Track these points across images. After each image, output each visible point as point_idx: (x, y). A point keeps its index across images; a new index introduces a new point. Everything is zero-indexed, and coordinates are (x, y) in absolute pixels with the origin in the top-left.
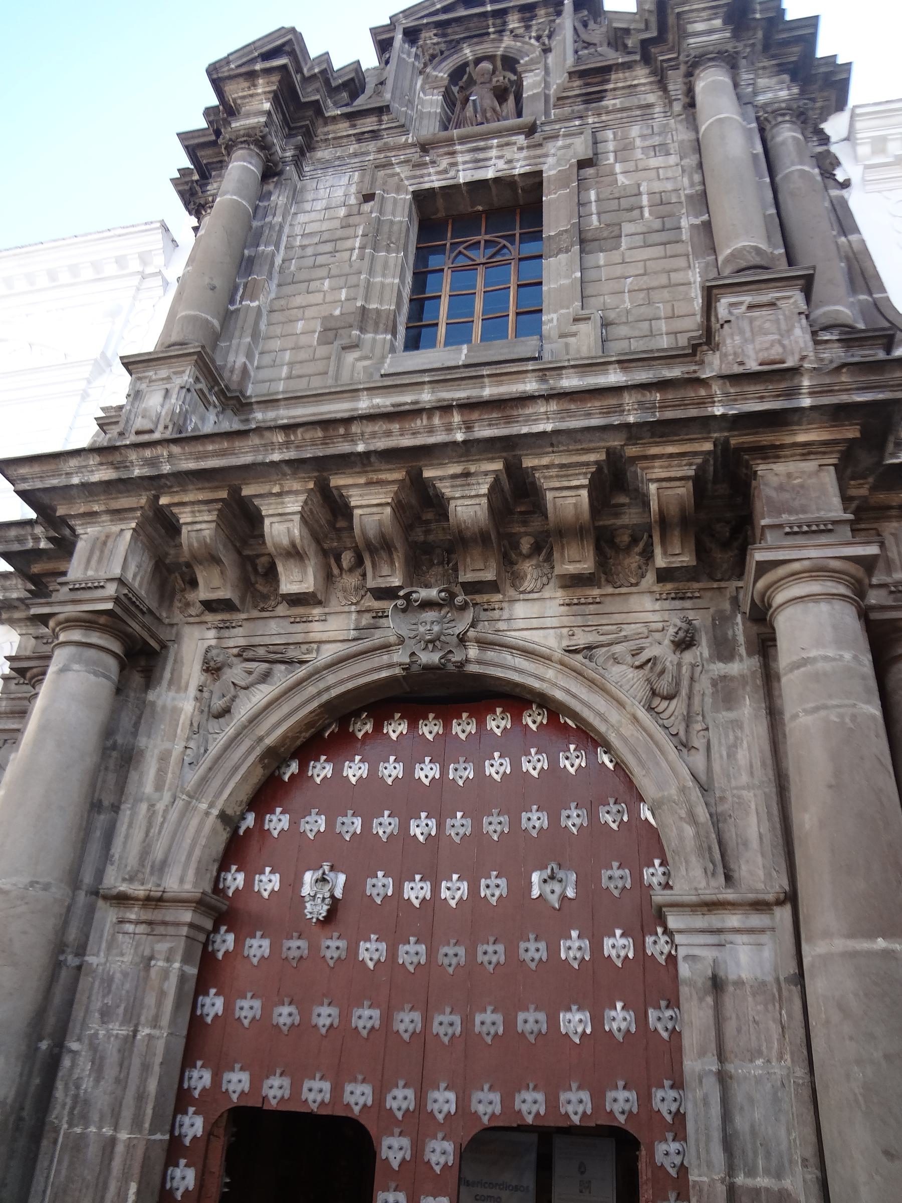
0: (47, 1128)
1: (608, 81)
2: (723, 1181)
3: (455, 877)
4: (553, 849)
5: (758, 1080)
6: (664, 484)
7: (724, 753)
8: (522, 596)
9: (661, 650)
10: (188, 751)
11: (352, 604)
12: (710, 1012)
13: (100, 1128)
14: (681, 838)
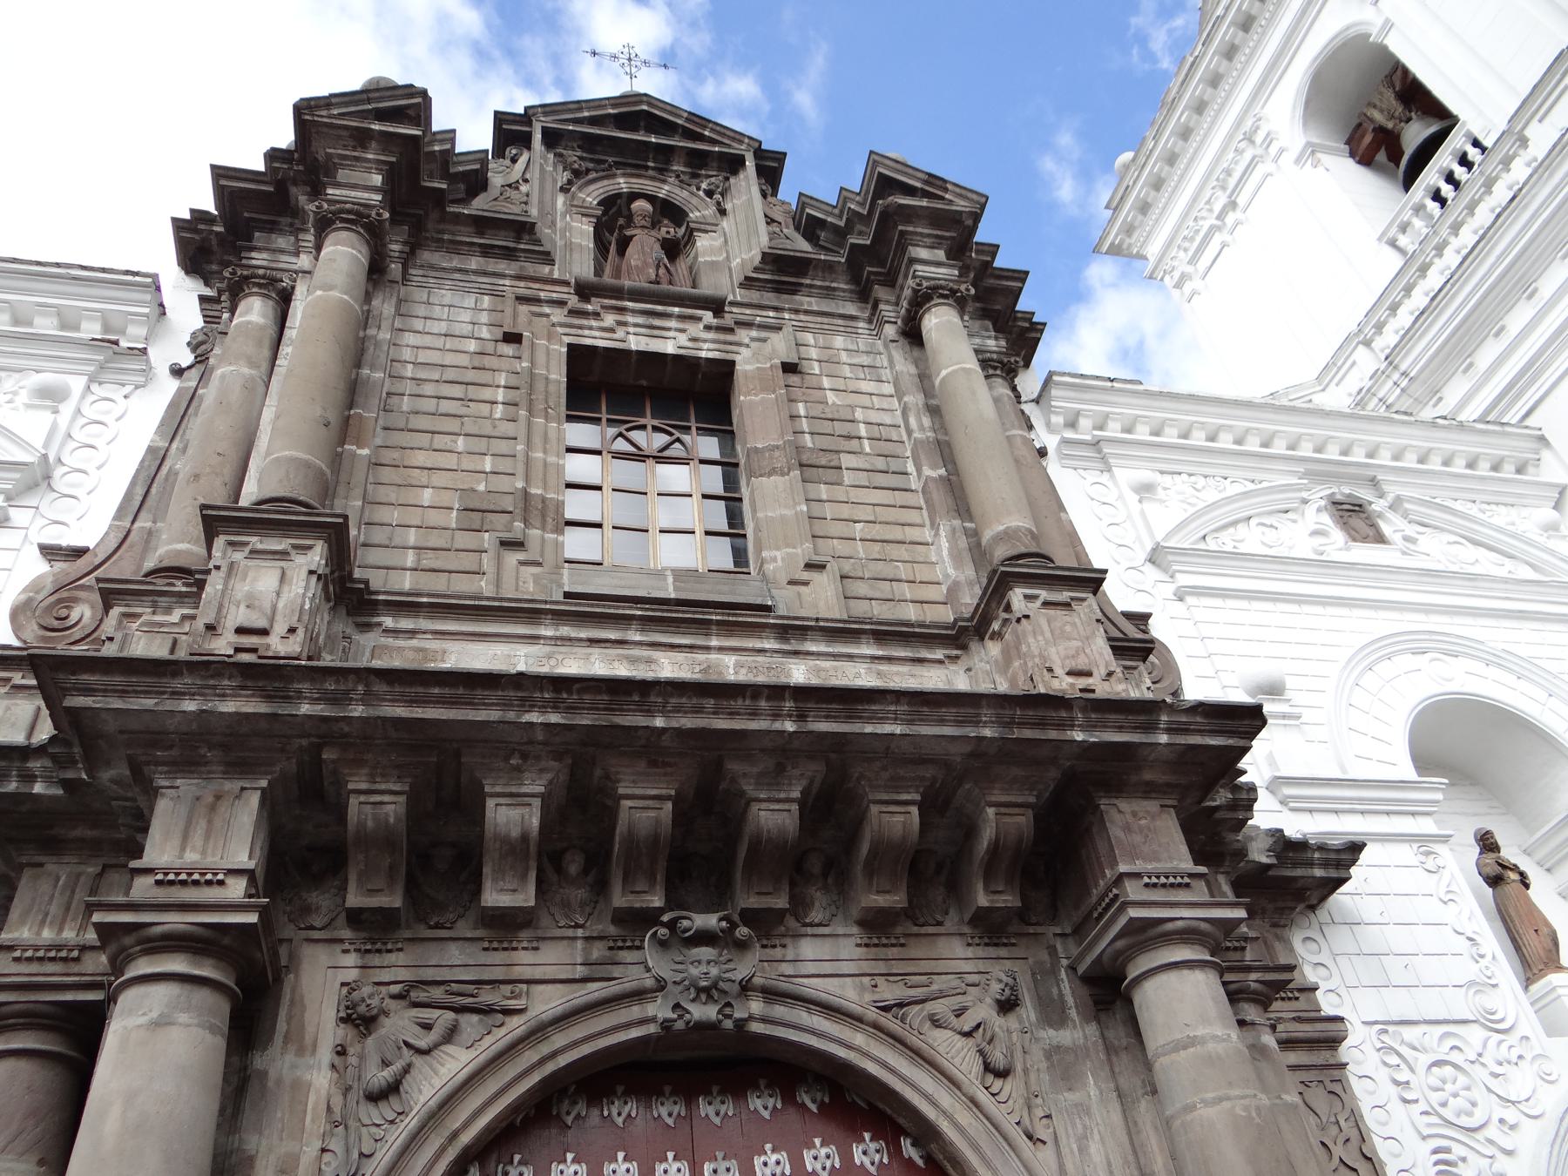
1: (804, 275)
6: (1003, 810)
7: (1075, 1147)
8: (809, 930)
9: (983, 1011)
10: (327, 1157)
11: (577, 926)
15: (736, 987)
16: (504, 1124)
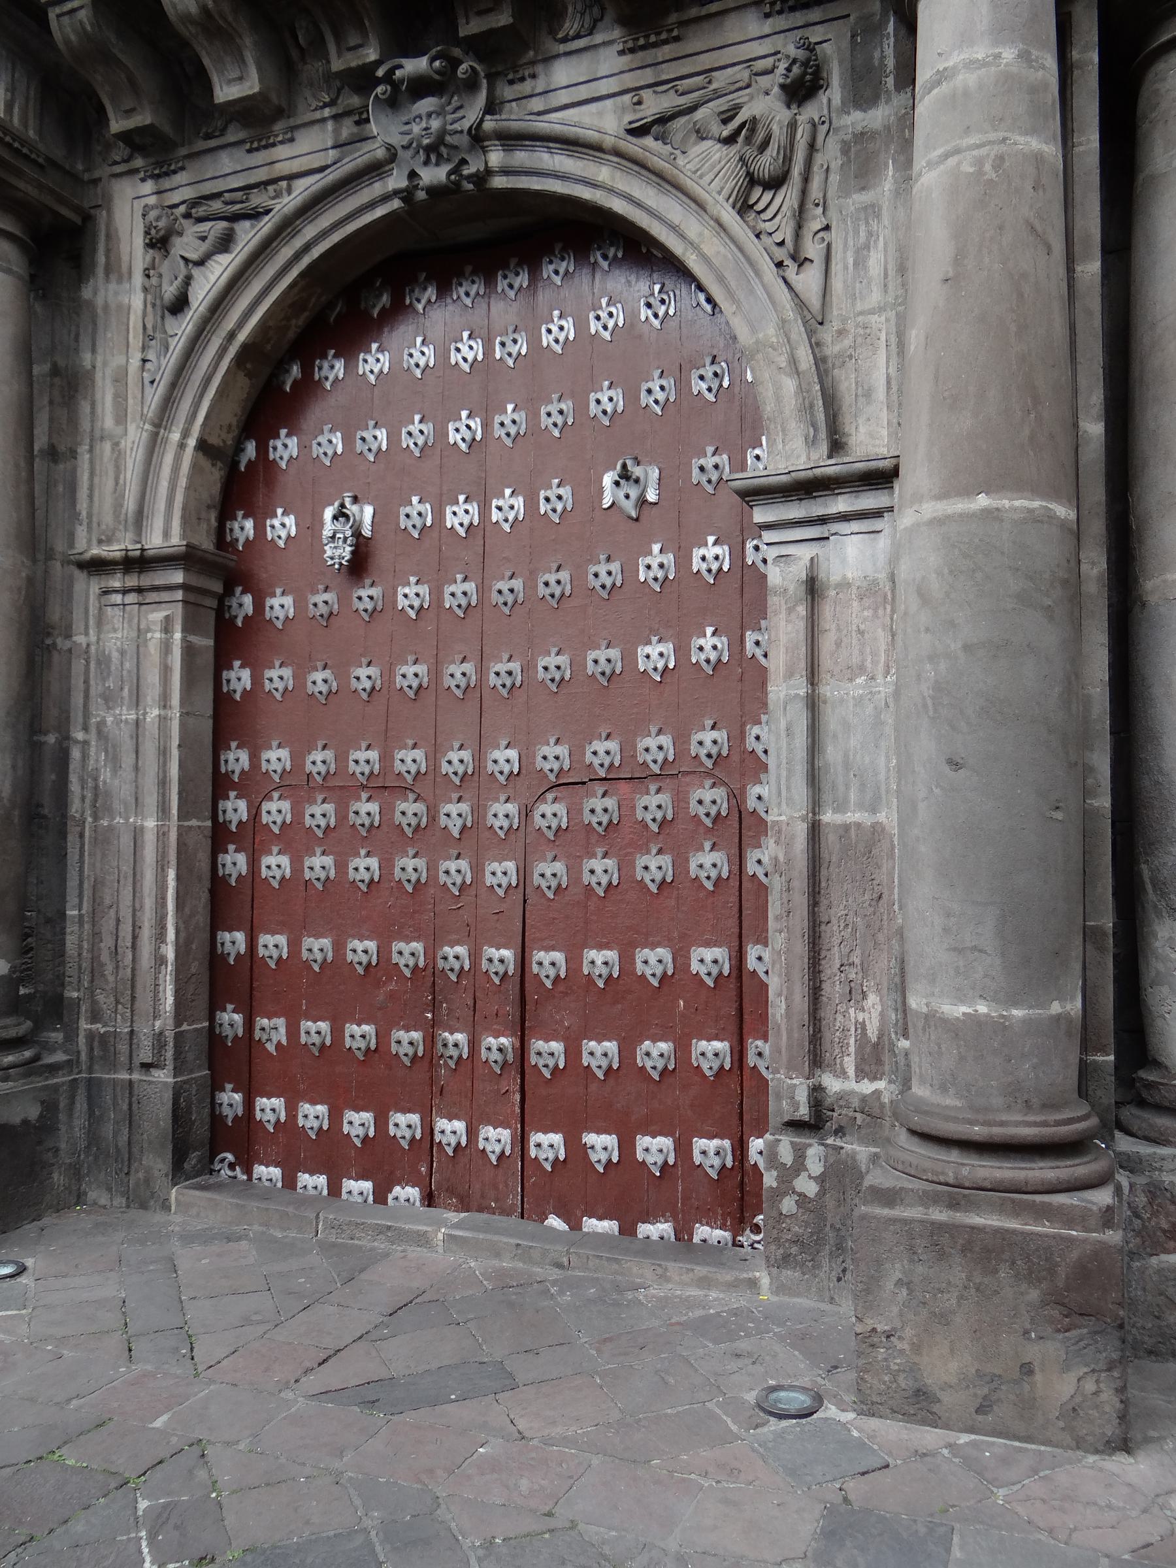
2: (804, 819)
4: (626, 440)
5: (859, 701)
7: (851, 261)
8: (562, 48)
9: (765, 105)
10: (148, 365)
11: (325, 105)
12: (801, 625)
13: (127, 819)
14: (778, 398)
15: (465, 140)
16: (300, 321)
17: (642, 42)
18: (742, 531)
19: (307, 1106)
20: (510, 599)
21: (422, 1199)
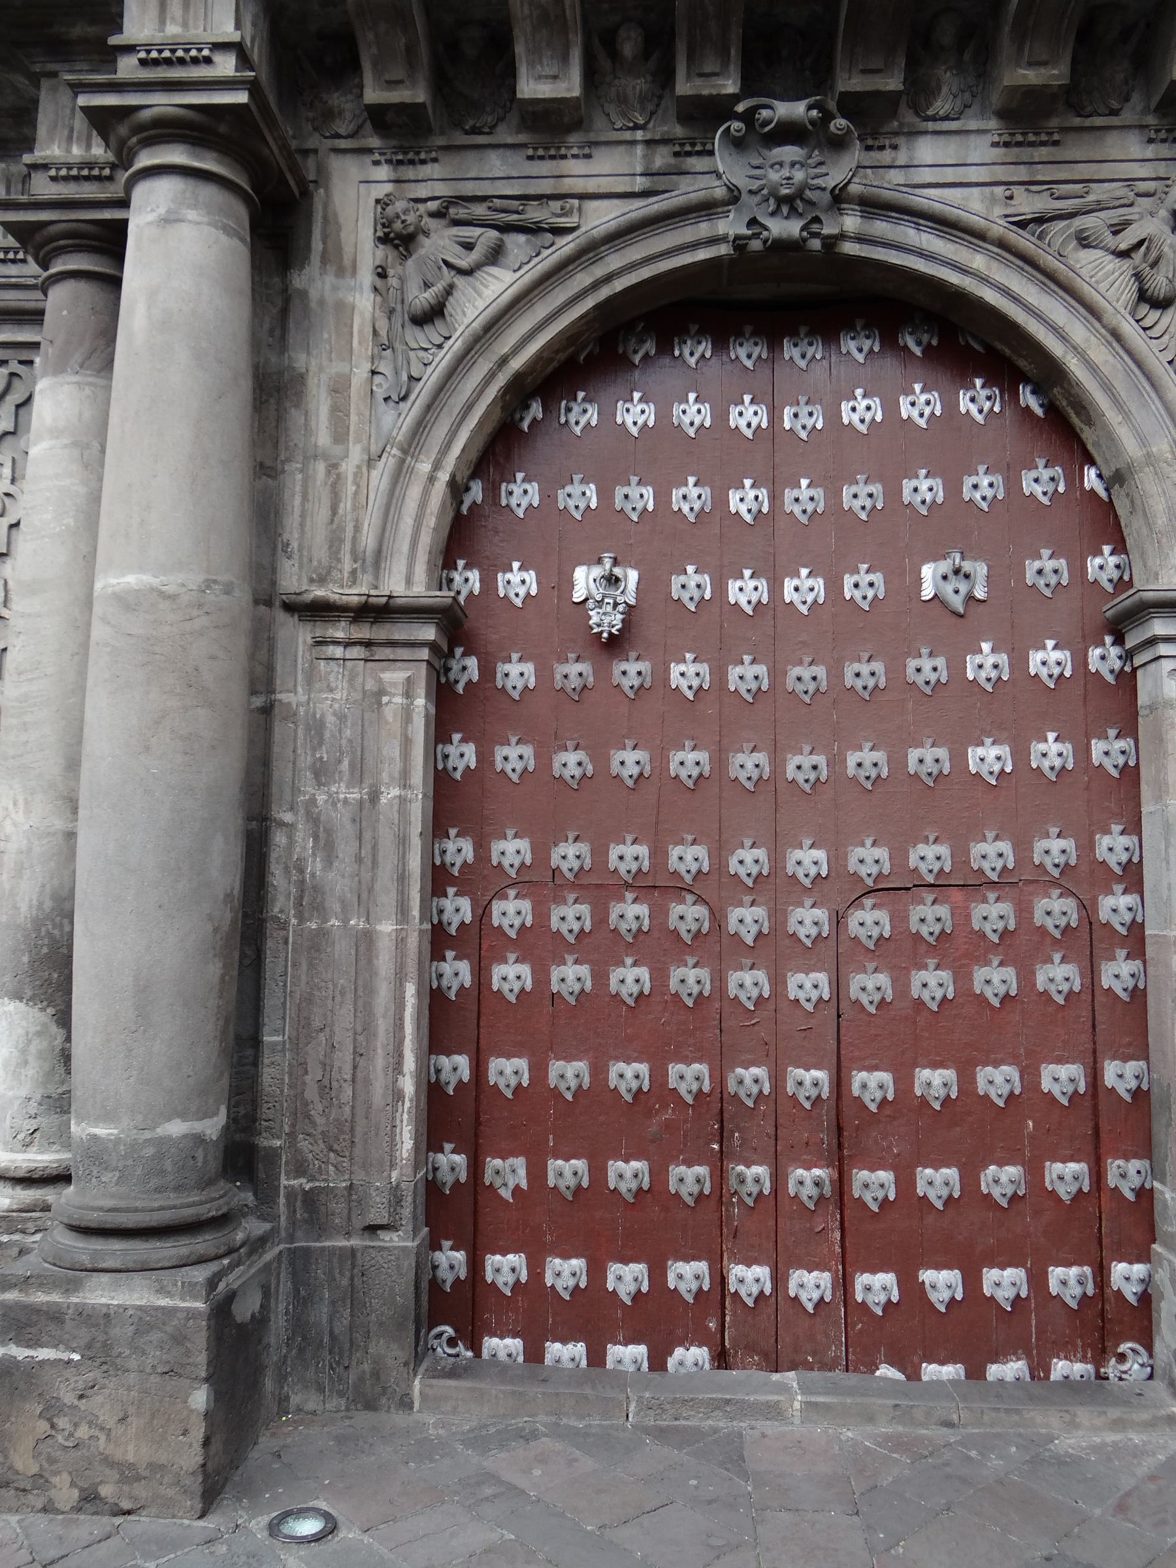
0: (270, 925)
3: (804, 572)
8: (931, 126)
10: (378, 379)
11: (636, 127)
13: (346, 921)
15: (826, 197)
16: (562, 357)
17: (1019, 138)
18: (1084, 637)
19: (557, 1261)
20: (812, 687)
21: (713, 1359)
